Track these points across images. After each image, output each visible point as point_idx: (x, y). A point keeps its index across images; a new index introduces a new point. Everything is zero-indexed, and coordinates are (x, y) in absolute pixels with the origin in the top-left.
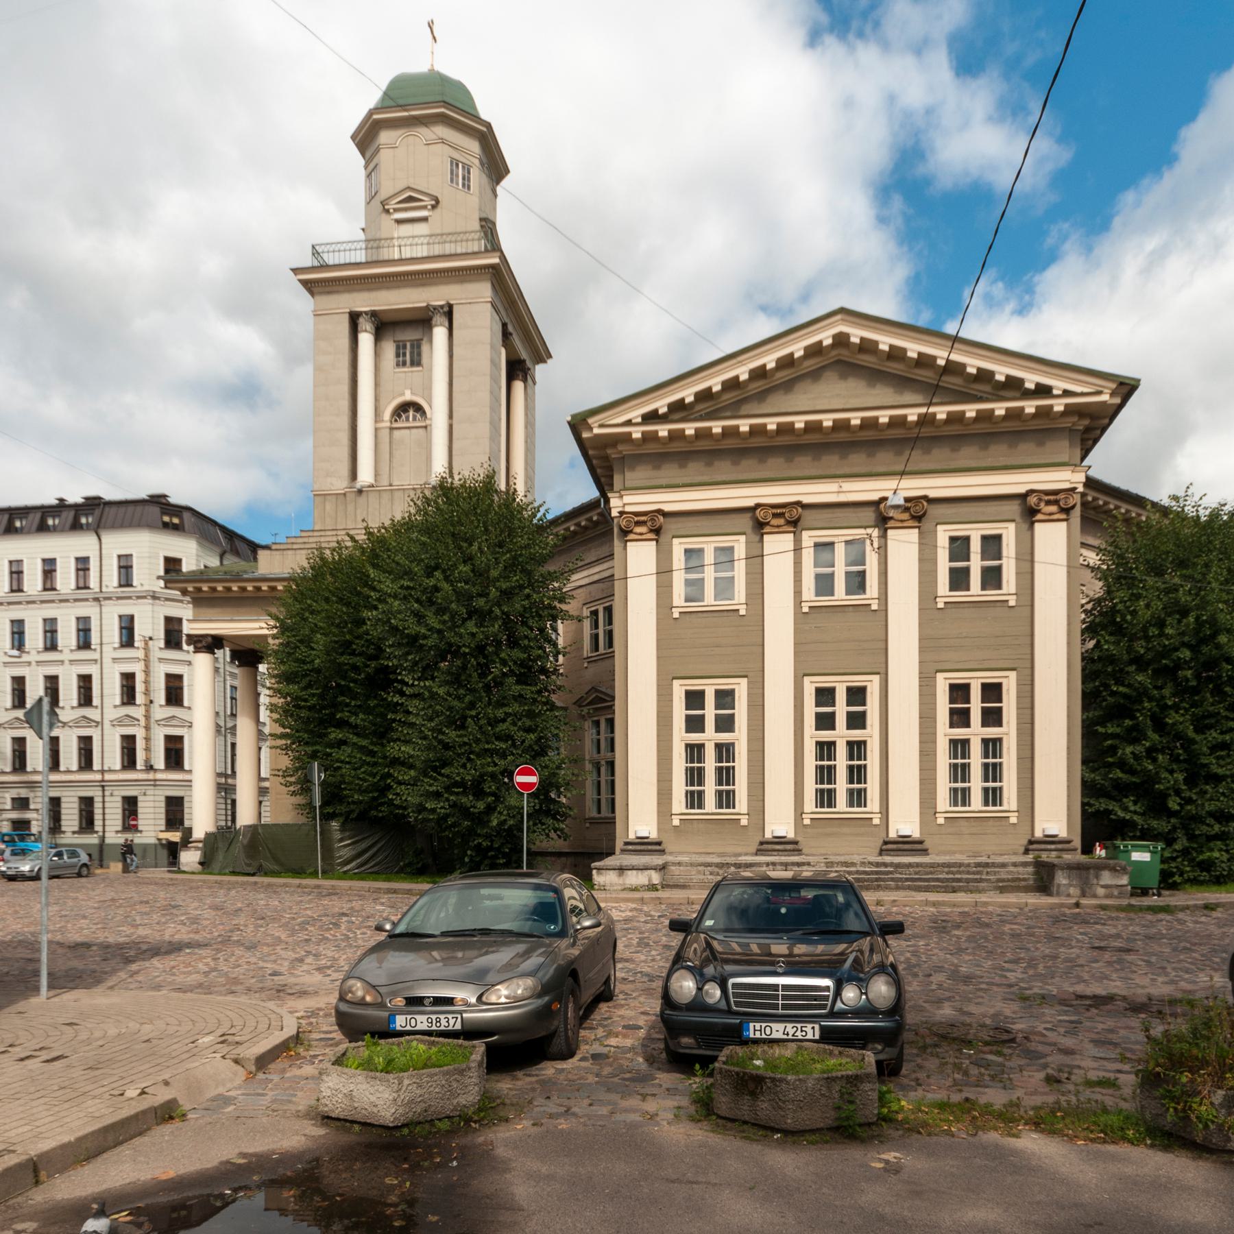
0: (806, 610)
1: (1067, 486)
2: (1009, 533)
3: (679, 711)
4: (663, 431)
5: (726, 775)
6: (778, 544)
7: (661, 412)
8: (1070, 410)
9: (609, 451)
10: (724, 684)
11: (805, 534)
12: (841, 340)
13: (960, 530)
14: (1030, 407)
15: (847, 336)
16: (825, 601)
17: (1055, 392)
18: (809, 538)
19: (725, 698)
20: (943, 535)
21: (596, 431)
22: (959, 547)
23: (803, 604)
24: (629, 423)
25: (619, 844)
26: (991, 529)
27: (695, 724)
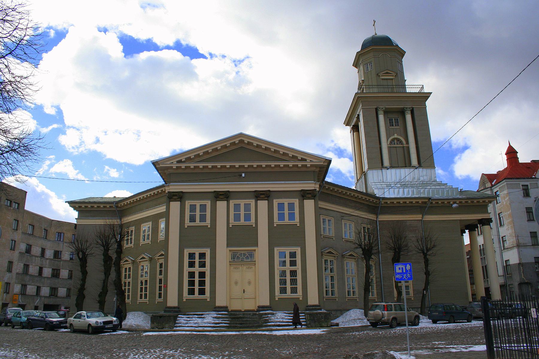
0: (231, 226)
1: (313, 189)
4: (183, 166)
6: (221, 205)
7: (183, 160)
8: (312, 166)
9: (166, 171)
10: (202, 250)
11: (231, 201)
12: (241, 141)
14: (300, 164)
15: (244, 141)
18: (232, 203)
19: (202, 255)
20: (276, 202)
21: (161, 165)
27: (192, 265)
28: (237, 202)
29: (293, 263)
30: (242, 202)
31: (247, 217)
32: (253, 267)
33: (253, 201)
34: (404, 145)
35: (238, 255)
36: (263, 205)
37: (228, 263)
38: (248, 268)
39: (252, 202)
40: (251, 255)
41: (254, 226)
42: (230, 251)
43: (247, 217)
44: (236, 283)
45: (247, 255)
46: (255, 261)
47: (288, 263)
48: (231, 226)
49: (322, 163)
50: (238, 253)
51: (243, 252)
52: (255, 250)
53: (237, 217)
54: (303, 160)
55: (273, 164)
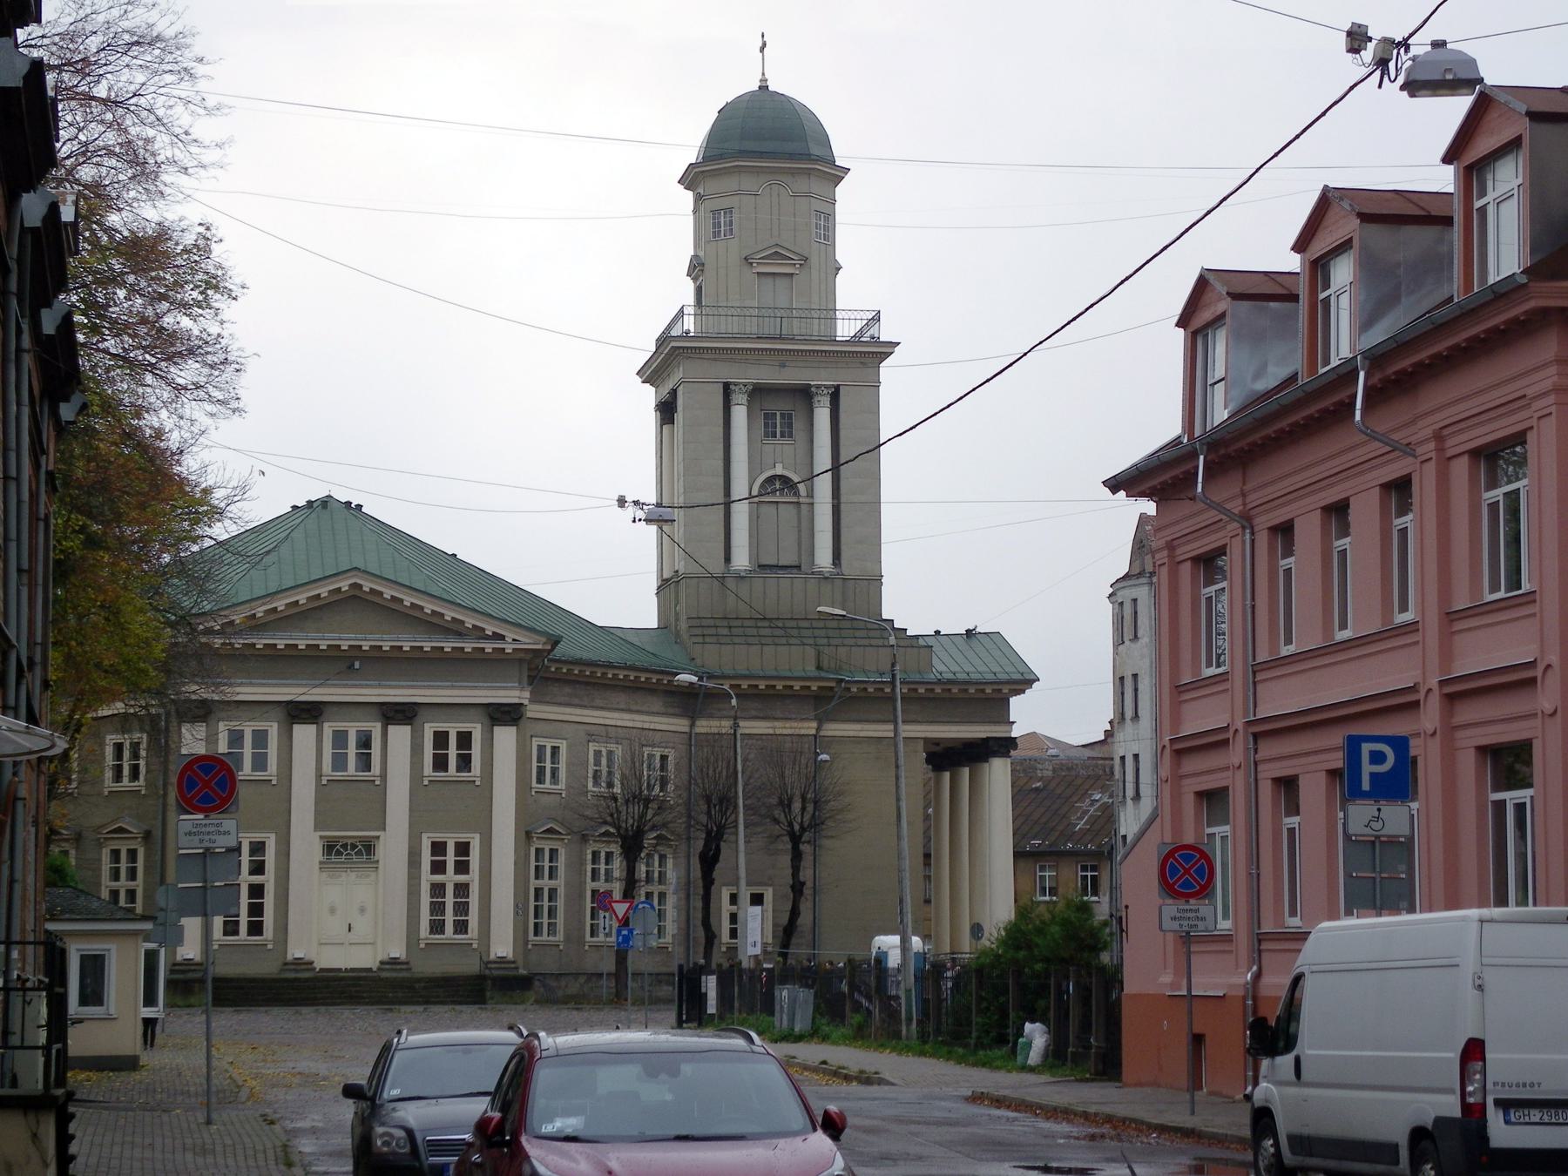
0: (324, 782)
6: (304, 734)
11: (326, 725)
13: (442, 727)
16: (339, 775)
18: (328, 729)
22: (441, 739)
26: (464, 727)
30: (353, 730)
32: (373, 874)
33: (379, 725)
34: (801, 500)
36: (400, 735)
37: (317, 867)
39: (376, 729)
40: (368, 847)
42: (321, 837)
44: (333, 911)
46: (378, 861)
47: (450, 867)
48: (324, 782)
51: (349, 842)
52: (378, 837)
53: (339, 762)
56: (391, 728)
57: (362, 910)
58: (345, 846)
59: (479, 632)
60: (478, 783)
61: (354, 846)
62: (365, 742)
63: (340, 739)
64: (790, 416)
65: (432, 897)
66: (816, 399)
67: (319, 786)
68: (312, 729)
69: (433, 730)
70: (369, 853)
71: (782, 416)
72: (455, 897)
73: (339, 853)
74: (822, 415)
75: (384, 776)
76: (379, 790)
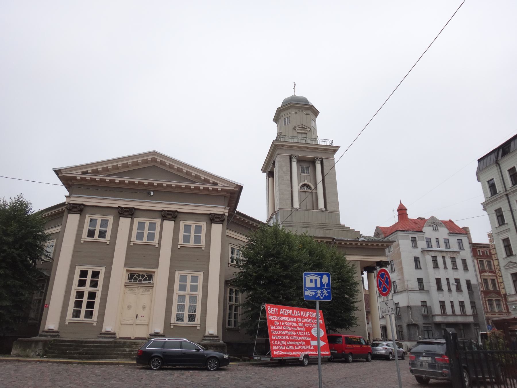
0: (132, 245)
1: (222, 213)
2: (204, 226)
3: (77, 277)
5: (90, 305)
6: (125, 222)
10: (96, 269)
11: (135, 219)
17: (219, 185)
18: (136, 221)
19: (96, 274)
20: (182, 224)
23: (131, 242)
24: (77, 173)
25: (40, 332)
27: (82, 283)
28: (142, 220)
29: (194, 288)
30: (147, 222)
31: (151, 236)
32: (151, 290)
33: (160, 220)
35: (136, 276)
36: (169, 225)
37: (123, 284)
38: (145, 291)
39: (158, 222)
40: (149, 277)
41: (157, 246)
42: (127, 271)
43: (151, 236)
44: (129, 307)
45: (146, 276)
46: (153, 284)
47: (188, 288)
49: (233, 189)
50: (136, 273)
51: (141, 274)
52: (154, 272)
53: (140, 236)
54: (214, 183)
55: (183, 185)
56: (165, 222)
57: (144, 308)
58: (139, 276)
59: (206, 181)
60: (203, 249)
61: (143, 276)
62: (152, 226)
63: (141, 225)
64: (308, 168)
65: (178, 302)
66: (316, 162)
67: (129, 246)
68: (129, 220)
69: (184, 224)
70: (150, 280)
71: (306, 168)
72: (190, 302)
73: (135, 279)
74: (318, 166)
75: (159, 244)
76: (156, 250)
